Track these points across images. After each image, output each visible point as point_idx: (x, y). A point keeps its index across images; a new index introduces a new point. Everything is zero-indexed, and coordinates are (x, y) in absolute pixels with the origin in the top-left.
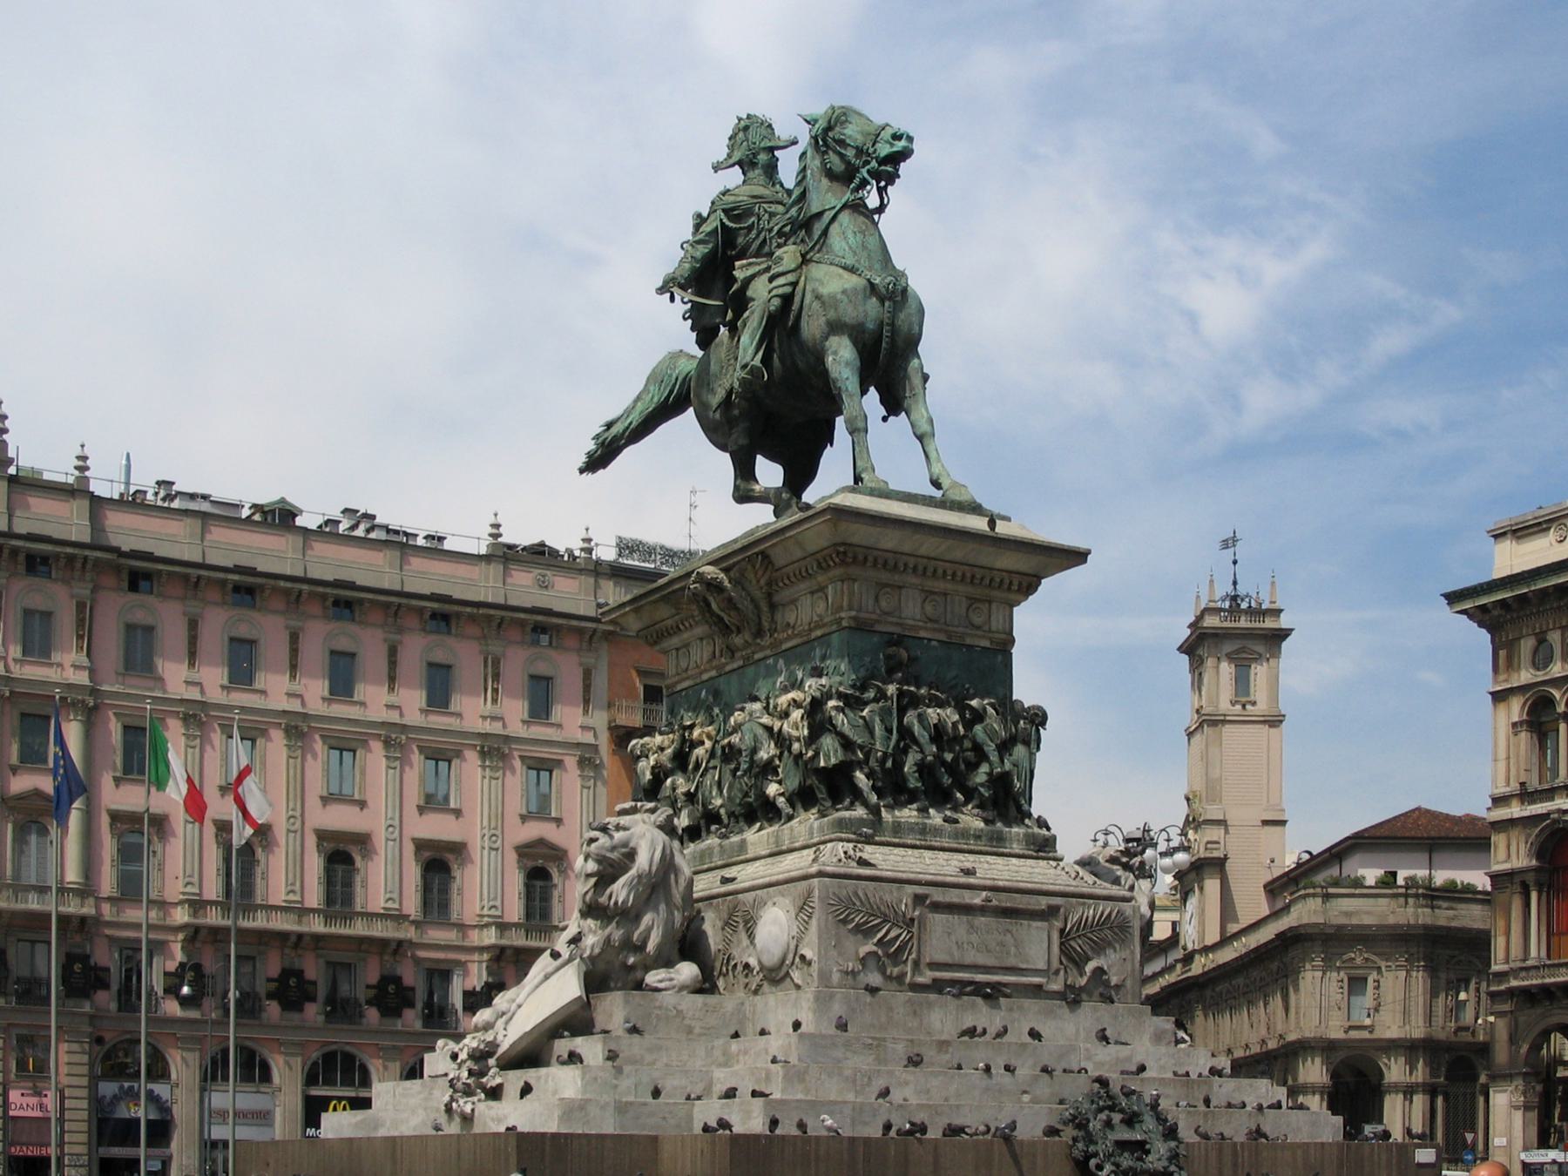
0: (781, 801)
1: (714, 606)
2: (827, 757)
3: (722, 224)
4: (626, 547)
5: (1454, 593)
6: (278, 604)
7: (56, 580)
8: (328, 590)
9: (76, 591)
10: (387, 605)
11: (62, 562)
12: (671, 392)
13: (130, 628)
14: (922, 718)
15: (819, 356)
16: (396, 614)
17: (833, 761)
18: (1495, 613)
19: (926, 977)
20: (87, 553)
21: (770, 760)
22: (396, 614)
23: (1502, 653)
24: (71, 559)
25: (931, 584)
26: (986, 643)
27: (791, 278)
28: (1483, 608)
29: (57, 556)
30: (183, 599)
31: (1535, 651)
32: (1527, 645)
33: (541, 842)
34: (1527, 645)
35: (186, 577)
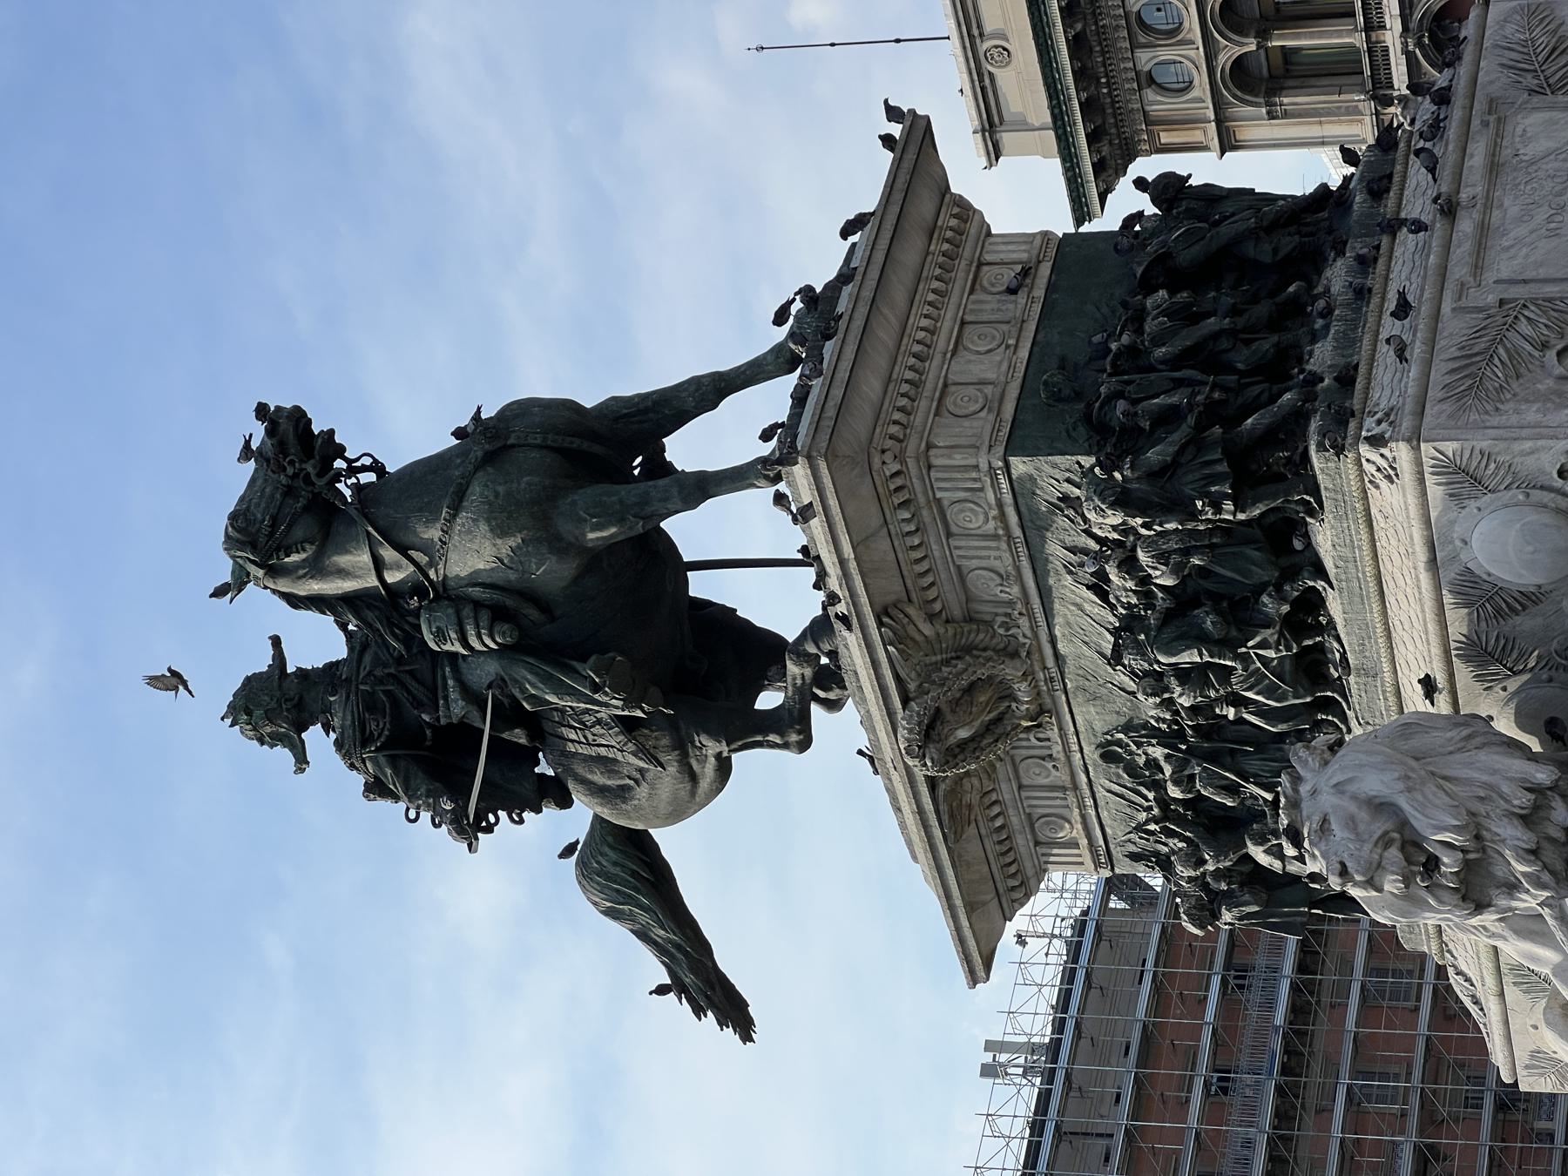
3: (378, 750)
5: (1074, 211)
14: (1158, 341)
15: (595, 559)
17: (1223, 468)
18: (1105, 150)
23: (1165, 138)
28: (1099, 168)
31: (1163, 89)
32: (1158, 104)
34: (1158, 104)
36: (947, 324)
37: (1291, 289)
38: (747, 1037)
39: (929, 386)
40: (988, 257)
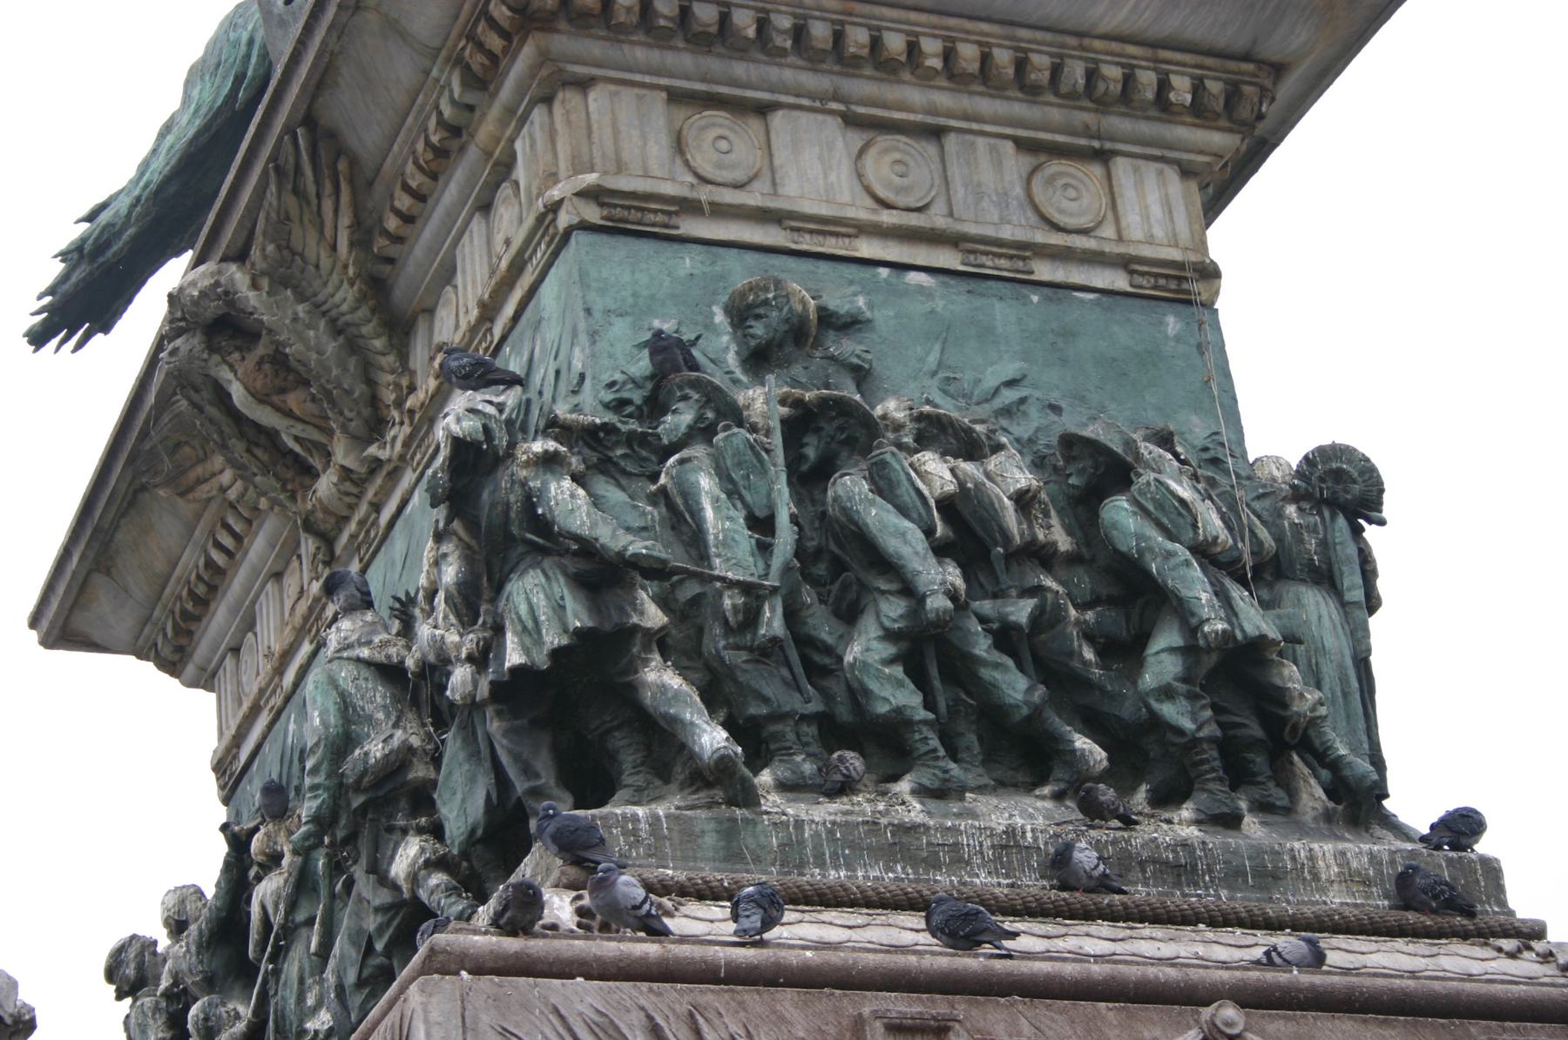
1: (237, 392)
2: (532, 632)
12: (239, 79)
17: (553, 638)
21: (400, 760)
36: (914, 95)
37: (1082, 742)
38: (38, 338)
39: (740, 69)
40: (1121, 166)
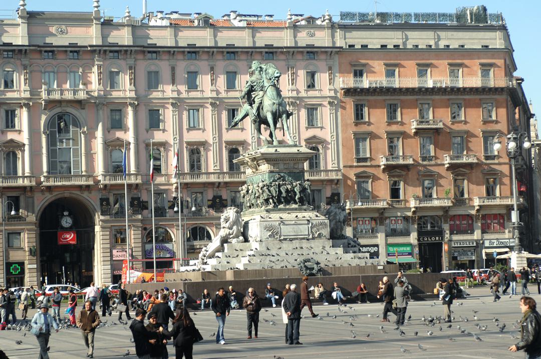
0: (260, 204)
4: (344, 15)
6: (205, 57)
7: (121, 59)
8: (224, 50)
9: (128, 62)
10: (247, 52)
11: (123, 52)
13: (149, 73)
16: (251, 55)
19: (282, 238)
20: (131, 48)
22: (251, 55)
24: (126, 51)
25: (285, 162)
26: (298, 171)
27: (261, 99)
29: (121, 51)
30: (169, 60)
33: (314, 137)
35: (169, 52)
